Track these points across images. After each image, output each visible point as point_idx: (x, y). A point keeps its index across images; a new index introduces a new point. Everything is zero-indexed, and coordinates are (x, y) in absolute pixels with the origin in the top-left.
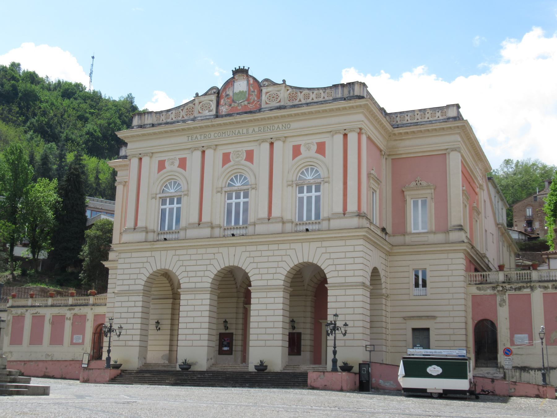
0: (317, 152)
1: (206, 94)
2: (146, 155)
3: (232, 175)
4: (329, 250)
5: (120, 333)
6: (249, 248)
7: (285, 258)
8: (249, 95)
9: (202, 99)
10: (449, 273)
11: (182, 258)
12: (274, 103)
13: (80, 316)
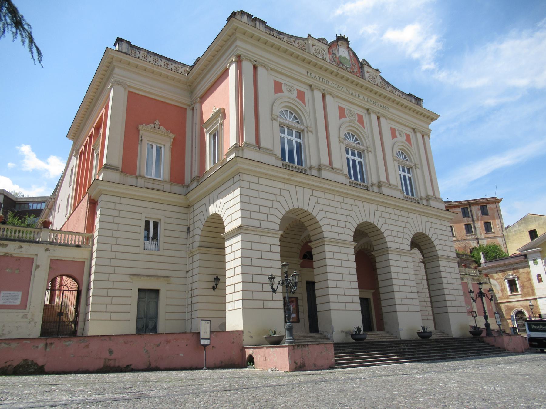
9: (316, 43)
13: (19, 259)
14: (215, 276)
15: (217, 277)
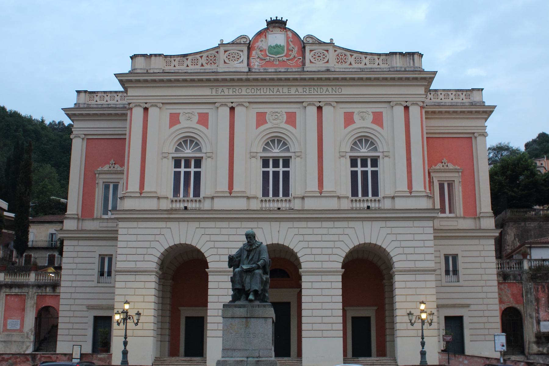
0: (373, 122)
1: (233, 43)
2: (154, 105)
4: (395, 231)
5: (138, 320)
6: (297, 224)
7: (342, 238)
8: (288, 50)
10: (481, 259)
11: (208, 231)
12: (236, 62)
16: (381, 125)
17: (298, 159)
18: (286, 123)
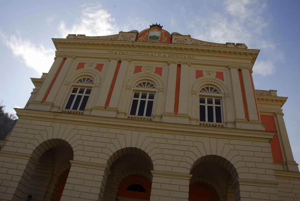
0: (216, 77)
3: (142, 80)
6: (153, 135)
8: (161, 38)
14: (29, 195)
15: (31, 195)
16: (223, 80)
17: (160, 93)
18: (155, 72)
